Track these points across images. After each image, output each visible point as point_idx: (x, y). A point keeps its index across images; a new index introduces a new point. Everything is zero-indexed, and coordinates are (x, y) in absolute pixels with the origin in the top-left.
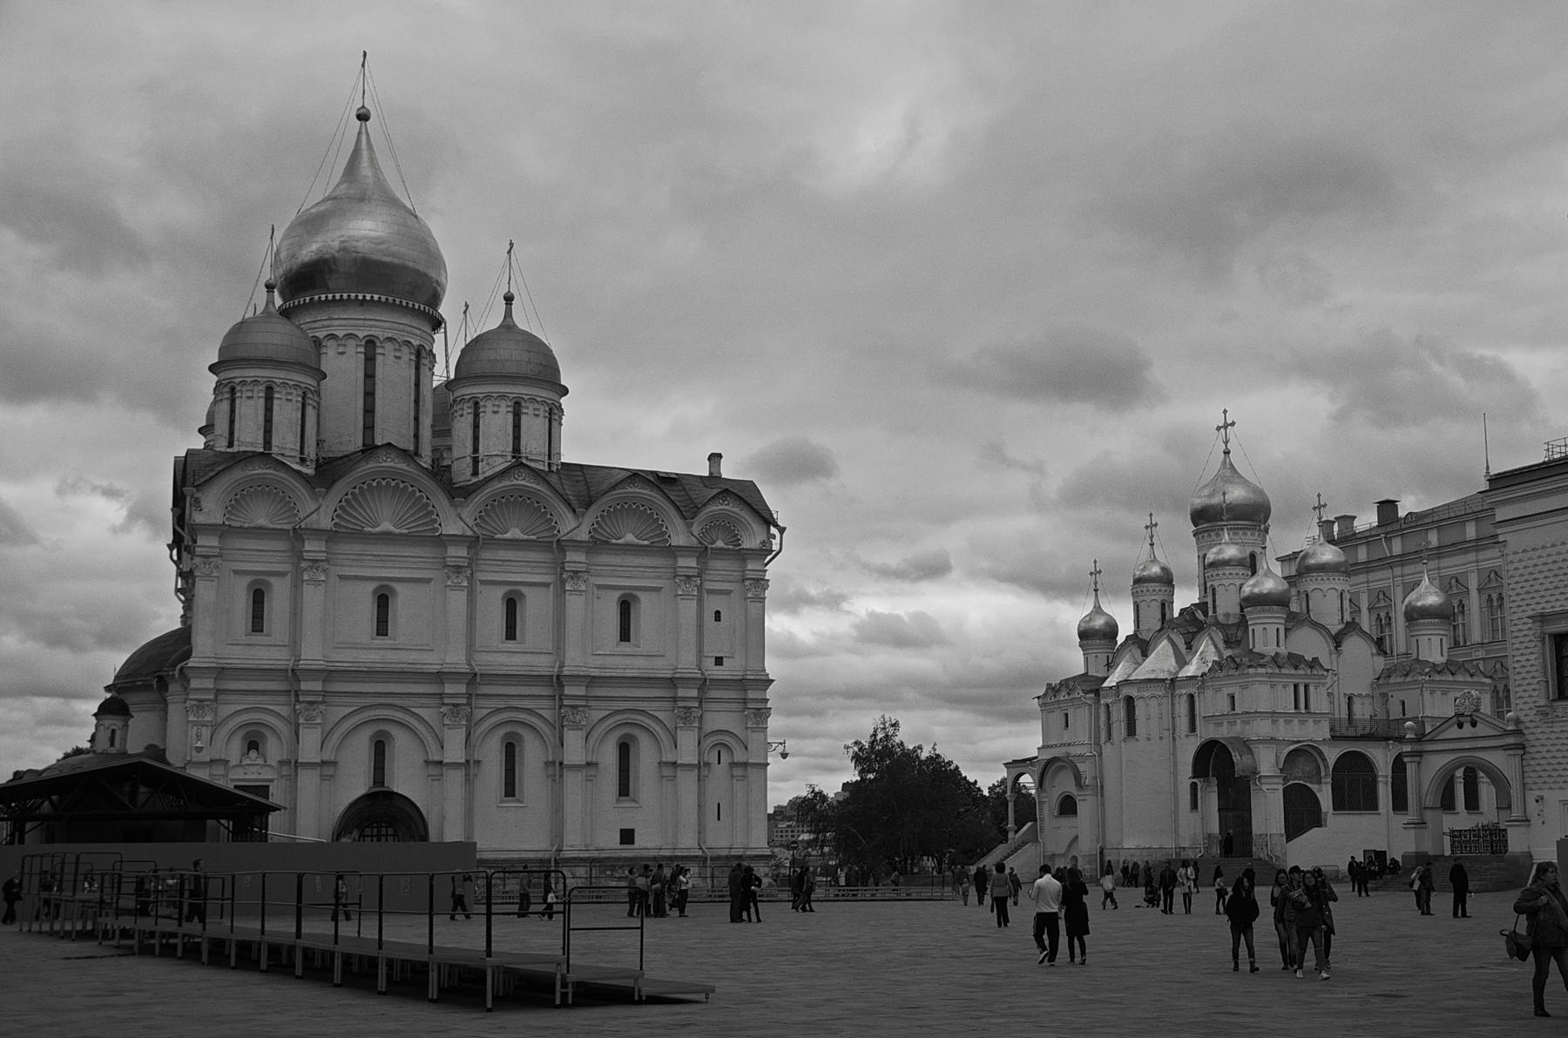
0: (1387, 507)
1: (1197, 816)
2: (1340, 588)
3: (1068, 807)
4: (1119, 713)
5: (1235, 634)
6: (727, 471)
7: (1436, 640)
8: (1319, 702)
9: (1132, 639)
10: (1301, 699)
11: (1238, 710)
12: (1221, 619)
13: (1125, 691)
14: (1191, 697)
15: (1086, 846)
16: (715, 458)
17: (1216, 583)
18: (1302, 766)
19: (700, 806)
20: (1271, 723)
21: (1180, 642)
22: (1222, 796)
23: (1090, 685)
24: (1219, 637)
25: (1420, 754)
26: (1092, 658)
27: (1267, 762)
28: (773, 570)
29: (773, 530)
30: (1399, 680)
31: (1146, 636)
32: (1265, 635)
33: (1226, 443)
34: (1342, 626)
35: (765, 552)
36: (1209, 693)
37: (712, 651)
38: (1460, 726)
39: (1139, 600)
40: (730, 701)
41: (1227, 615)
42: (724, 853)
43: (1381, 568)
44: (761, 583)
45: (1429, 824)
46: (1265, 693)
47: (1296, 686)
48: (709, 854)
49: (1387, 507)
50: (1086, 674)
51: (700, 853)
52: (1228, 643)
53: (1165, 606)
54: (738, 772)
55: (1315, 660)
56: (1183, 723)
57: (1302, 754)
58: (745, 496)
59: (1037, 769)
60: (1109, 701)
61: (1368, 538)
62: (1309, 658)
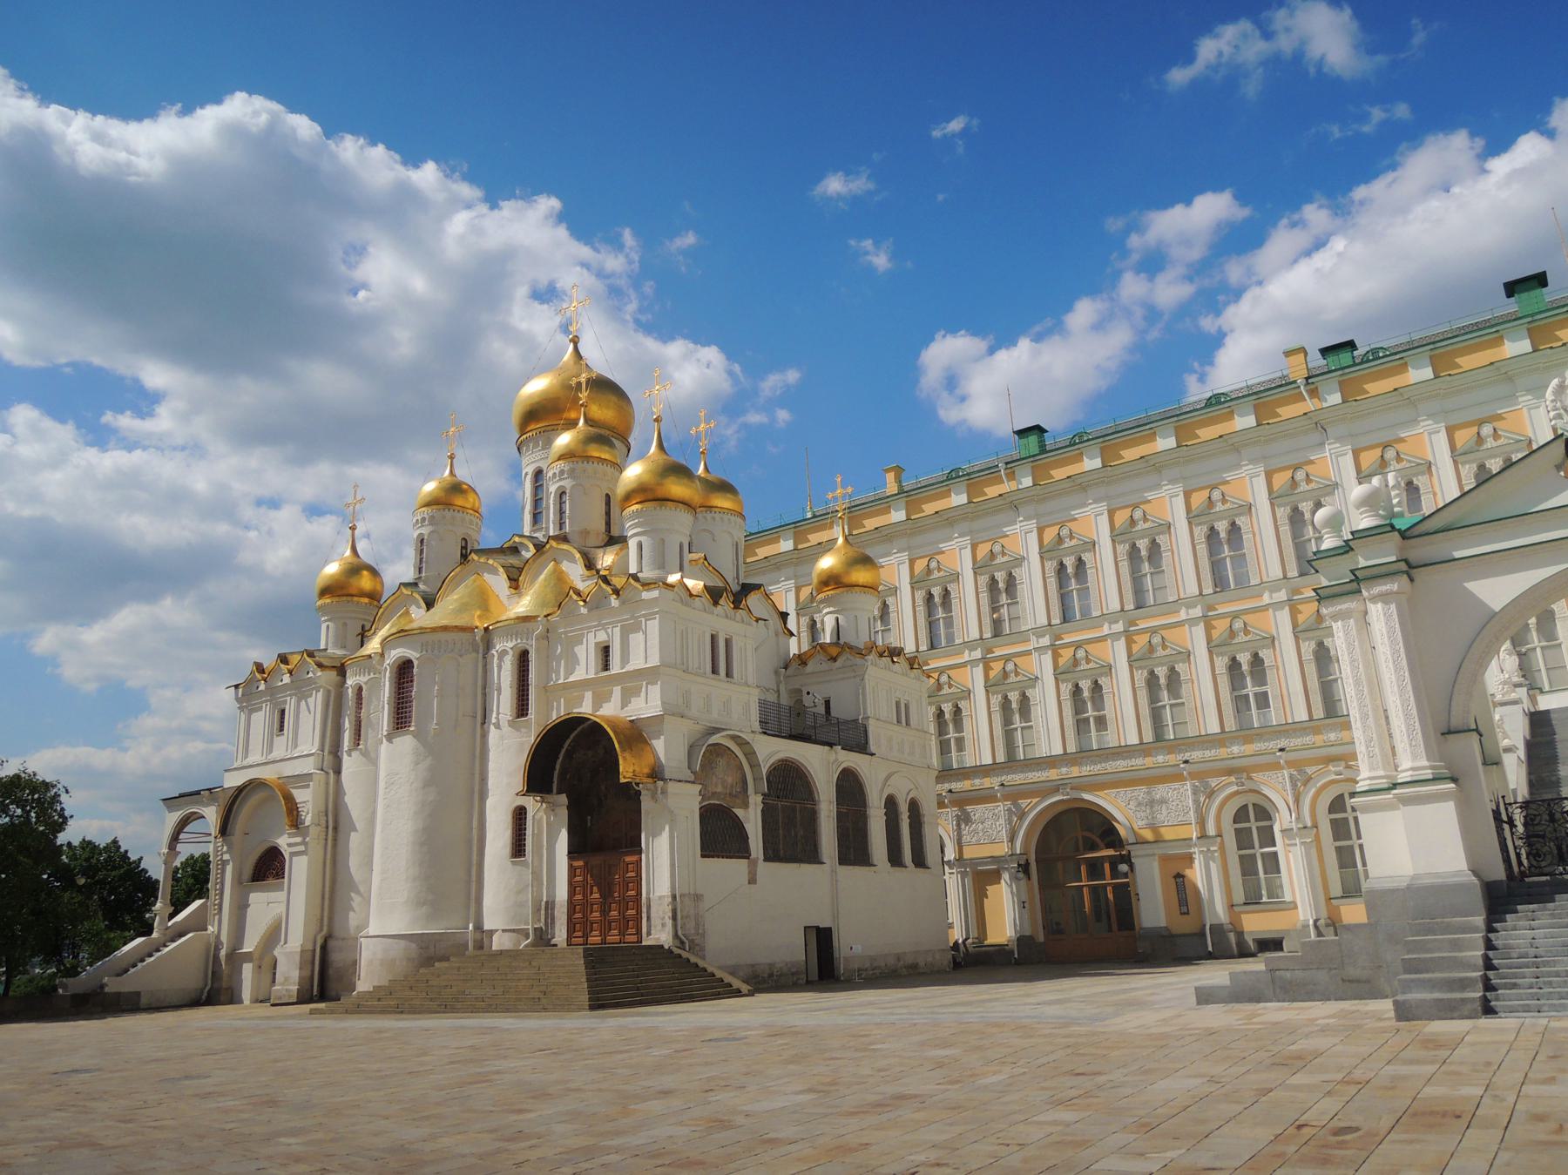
11: (615, 668)
14: (523, 658)
30: (826, 666)
60: (362, 679)
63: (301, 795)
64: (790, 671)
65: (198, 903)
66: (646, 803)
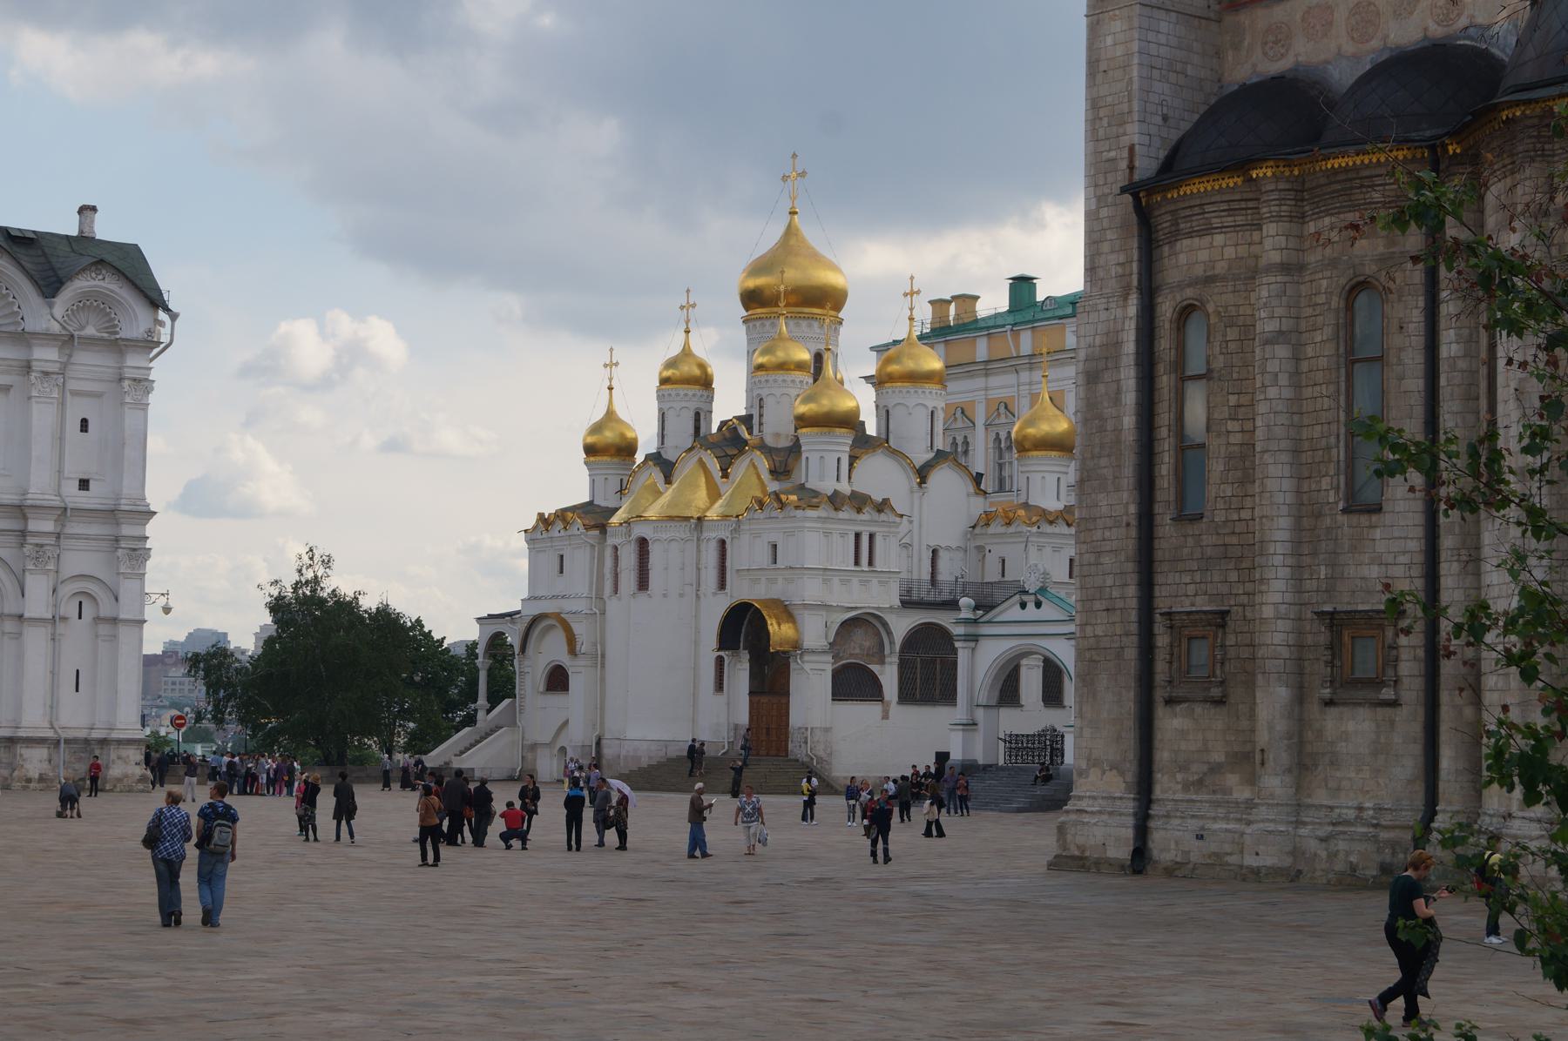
0: (1022, 285)
1: (721, 699)
2: (930, 404)
3: (557, 680)
4: (629, 558)
5: (785, 461)
6: (106, 230)
7: (1051, 480)
8: (889, 556)
9: (656, 458)
10: (864, 550)
12: (769, 441)
13: (640, 531)
14: (723, 543)
15: (578, 736)
16: (87, 211)
17: (764, 393)
18: (860, 642)
19: (54, 673)
20: (822, 580)
21: (714, 466)
22: (753, 676)
23: (594, 516)
24: (764, 464)
25: (974, 638)
26: (600, 480)
27: (815, 632)
28: (161, 369)
29: (162, 315)
30: (1002, 530)
31: (670, 455)
32: (824, 464)
33: (793, 199)
34: (931, 455)
35: (149, 344)
36: (745, 538)
37: (74, 471)
38: (1023, 605)
39: (666, 406)
40: (96, 538)
41: (777, 435)
42: (82, 734)
43: (1003, 371)
44: (143, 384)
45: (981, 726)
46: (818, 544)
47: (858, 536)
48: (64, 735)
49: (1022, 285)
50: (591, 503)
51: (50, 734)
52: (774, 473)
53: (700, 418)
54: (104, 629)
55: (886, 502)
56: (710, 576)
57: (860, 623)
58: (128, 266)
59: (520, 627)
61: (990, 327)
62: (878, 498)
63: (579, 628)
64: (977, 530)
65: (507, 701)
66: (793, 666)
